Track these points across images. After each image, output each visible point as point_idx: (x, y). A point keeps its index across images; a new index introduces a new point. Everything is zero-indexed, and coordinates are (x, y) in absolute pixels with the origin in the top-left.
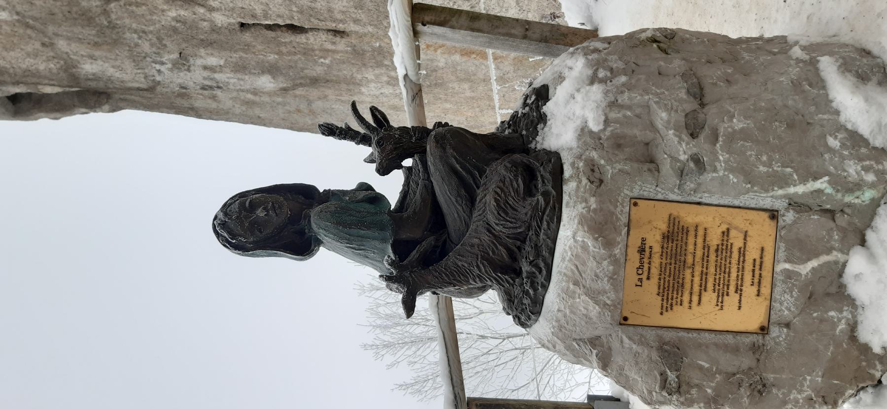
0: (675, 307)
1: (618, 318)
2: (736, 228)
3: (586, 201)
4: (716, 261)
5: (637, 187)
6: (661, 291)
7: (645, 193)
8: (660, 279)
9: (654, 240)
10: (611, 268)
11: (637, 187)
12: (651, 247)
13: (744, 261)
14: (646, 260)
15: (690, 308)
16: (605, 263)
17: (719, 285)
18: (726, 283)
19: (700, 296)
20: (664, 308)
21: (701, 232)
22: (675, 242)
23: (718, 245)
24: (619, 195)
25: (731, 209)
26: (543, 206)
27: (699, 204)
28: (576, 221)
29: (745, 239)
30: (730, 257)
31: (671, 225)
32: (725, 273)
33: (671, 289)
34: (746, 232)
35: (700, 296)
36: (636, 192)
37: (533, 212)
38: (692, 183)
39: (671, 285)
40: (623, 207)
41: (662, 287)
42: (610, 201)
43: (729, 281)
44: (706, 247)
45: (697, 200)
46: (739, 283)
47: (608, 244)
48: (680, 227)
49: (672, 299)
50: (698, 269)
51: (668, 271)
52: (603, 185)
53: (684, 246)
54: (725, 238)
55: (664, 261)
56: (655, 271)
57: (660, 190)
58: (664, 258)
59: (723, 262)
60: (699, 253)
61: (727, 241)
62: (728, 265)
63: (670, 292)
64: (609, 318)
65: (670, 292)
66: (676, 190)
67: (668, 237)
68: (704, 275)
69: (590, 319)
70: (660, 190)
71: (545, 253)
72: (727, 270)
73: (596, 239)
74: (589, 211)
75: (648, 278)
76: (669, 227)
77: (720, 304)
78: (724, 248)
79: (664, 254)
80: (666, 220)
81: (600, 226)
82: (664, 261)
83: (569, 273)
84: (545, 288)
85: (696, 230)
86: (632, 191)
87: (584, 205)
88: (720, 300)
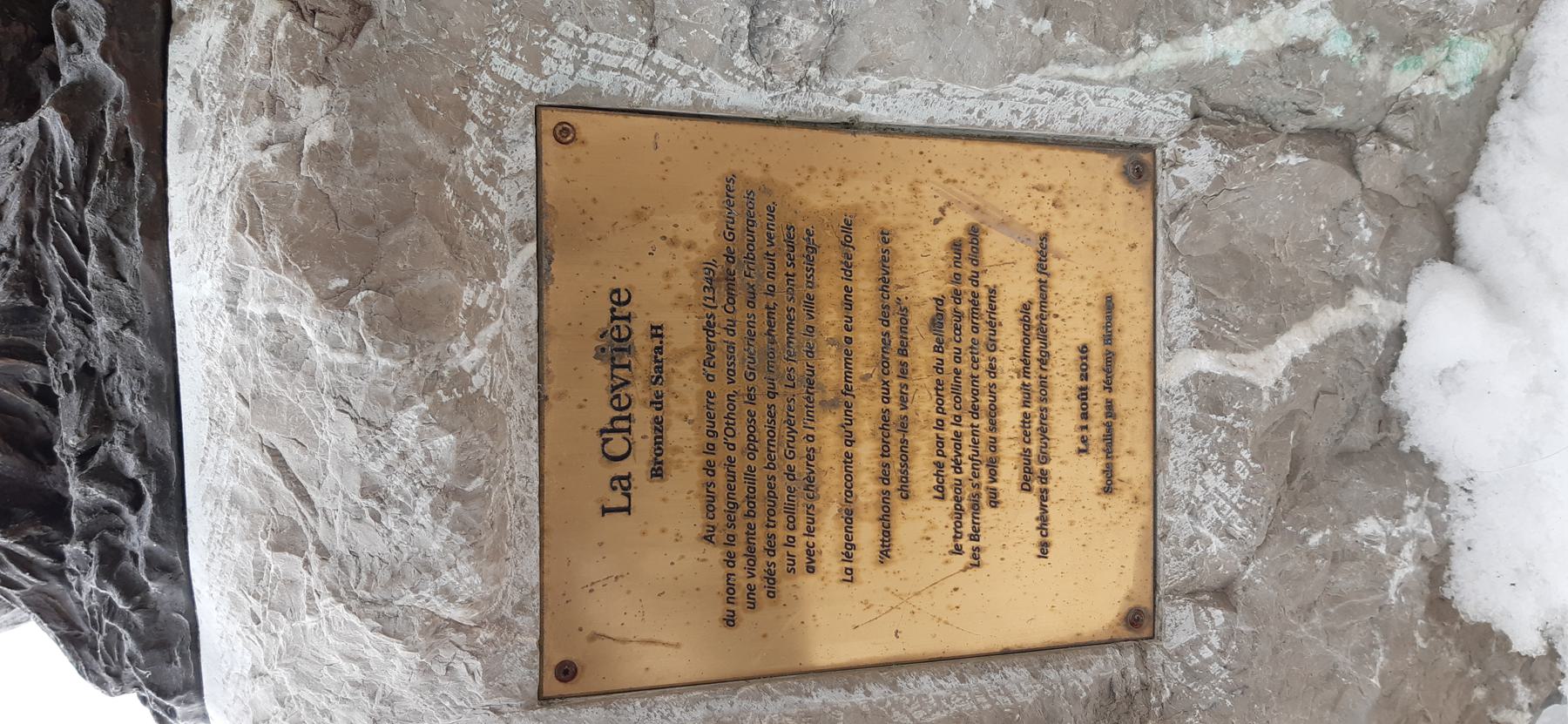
0: (784, 585)
1: (522, 675)
2: (1005, 224)
3: (275, 106)
4: (939, 368)
5: (560, 48)
6: (721, 519)
7: (605, 80)
8: (709, 468)
9: (668, 298)
10: (444, 443)
11: (560, 48)
12: (657, 331)
13: (1044, 361)
14: (639, 391)
15: (849, 576)
16: (408, 421)
17: (957, 467)
18: (985, 453)
19: (885, 519)
20: (740, 595)
21: (867, 249)
22: (762, 301)
23: (939, 301)
24: (467, 81)
25: (978, 147)
26: (73, 163)
27: (850, 126)
28: (228, 216)
29: (1042, 267)
30: (992, 345)
31: (740, 224)
32: (975, 412)
33: (761, 508)
34: (1045, 237)
35: (885, 519)
36: (558, 78)
37: (28, 198)
38: (804, 16)
39: (762, 489)
40: (500, 142)
41: (721, 505)
42: (418, 111)
43: (993, 444)
44: (893, 311)
45: (834, 105)
46: (1034, 447)
47: (407, 321)
48: (780, 234)
49: (771, 550)
50: (867, 407)
51: (742, 429)
52: (369, 31)
53: (801, 311)
54: (967, 268)
55: (721, 388)
56: (683, 435)
57: (670, 62)
58: (721, 373)
59: (965, 367)
60: (866, 340)
61: (975, 280)
62: (985, 381)
63: (760, 520)
64: (476, 687)
65: (760, 520)
66: (741, 61)
67: (730, 277)
68: (894, 430)
69: (390, 700)
70: (670, 62)
71: (133, 406)
72: (984, 401)
73: (337, 301)
74: (293, 157)
75: (657, 472)
76: (729, 234)
77: (967, 545)
78: (964, 309)
79: (720, 356)
80: (714, 203)
81: (359, 240)
82: (721, 388)
83: (252, 494)
84: (175, 571)
85: (847, 243)
86: (535, 67)
87: (263, 126)
88: (967, 528)
